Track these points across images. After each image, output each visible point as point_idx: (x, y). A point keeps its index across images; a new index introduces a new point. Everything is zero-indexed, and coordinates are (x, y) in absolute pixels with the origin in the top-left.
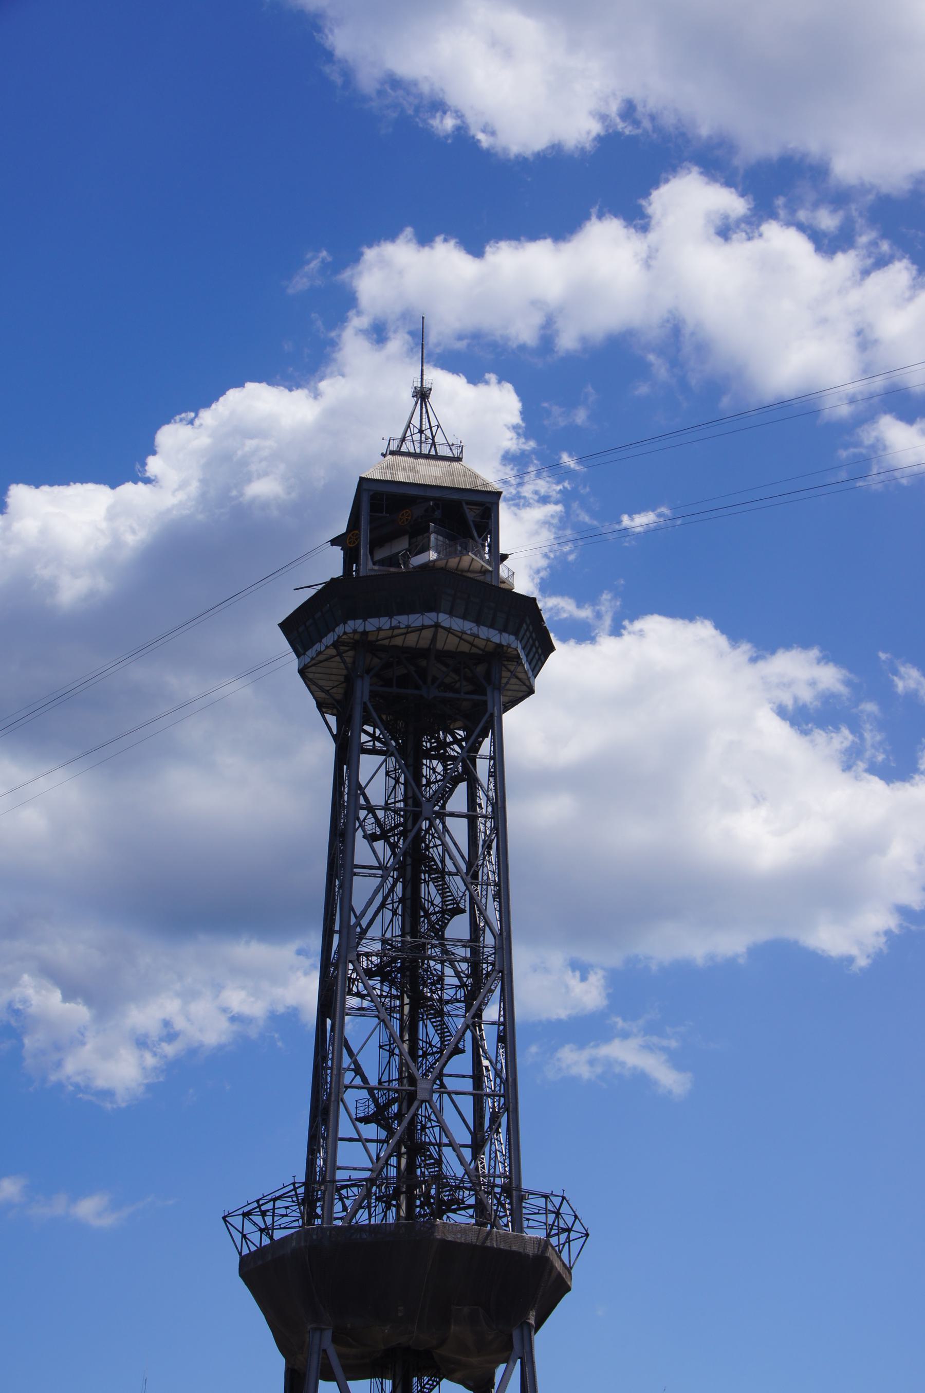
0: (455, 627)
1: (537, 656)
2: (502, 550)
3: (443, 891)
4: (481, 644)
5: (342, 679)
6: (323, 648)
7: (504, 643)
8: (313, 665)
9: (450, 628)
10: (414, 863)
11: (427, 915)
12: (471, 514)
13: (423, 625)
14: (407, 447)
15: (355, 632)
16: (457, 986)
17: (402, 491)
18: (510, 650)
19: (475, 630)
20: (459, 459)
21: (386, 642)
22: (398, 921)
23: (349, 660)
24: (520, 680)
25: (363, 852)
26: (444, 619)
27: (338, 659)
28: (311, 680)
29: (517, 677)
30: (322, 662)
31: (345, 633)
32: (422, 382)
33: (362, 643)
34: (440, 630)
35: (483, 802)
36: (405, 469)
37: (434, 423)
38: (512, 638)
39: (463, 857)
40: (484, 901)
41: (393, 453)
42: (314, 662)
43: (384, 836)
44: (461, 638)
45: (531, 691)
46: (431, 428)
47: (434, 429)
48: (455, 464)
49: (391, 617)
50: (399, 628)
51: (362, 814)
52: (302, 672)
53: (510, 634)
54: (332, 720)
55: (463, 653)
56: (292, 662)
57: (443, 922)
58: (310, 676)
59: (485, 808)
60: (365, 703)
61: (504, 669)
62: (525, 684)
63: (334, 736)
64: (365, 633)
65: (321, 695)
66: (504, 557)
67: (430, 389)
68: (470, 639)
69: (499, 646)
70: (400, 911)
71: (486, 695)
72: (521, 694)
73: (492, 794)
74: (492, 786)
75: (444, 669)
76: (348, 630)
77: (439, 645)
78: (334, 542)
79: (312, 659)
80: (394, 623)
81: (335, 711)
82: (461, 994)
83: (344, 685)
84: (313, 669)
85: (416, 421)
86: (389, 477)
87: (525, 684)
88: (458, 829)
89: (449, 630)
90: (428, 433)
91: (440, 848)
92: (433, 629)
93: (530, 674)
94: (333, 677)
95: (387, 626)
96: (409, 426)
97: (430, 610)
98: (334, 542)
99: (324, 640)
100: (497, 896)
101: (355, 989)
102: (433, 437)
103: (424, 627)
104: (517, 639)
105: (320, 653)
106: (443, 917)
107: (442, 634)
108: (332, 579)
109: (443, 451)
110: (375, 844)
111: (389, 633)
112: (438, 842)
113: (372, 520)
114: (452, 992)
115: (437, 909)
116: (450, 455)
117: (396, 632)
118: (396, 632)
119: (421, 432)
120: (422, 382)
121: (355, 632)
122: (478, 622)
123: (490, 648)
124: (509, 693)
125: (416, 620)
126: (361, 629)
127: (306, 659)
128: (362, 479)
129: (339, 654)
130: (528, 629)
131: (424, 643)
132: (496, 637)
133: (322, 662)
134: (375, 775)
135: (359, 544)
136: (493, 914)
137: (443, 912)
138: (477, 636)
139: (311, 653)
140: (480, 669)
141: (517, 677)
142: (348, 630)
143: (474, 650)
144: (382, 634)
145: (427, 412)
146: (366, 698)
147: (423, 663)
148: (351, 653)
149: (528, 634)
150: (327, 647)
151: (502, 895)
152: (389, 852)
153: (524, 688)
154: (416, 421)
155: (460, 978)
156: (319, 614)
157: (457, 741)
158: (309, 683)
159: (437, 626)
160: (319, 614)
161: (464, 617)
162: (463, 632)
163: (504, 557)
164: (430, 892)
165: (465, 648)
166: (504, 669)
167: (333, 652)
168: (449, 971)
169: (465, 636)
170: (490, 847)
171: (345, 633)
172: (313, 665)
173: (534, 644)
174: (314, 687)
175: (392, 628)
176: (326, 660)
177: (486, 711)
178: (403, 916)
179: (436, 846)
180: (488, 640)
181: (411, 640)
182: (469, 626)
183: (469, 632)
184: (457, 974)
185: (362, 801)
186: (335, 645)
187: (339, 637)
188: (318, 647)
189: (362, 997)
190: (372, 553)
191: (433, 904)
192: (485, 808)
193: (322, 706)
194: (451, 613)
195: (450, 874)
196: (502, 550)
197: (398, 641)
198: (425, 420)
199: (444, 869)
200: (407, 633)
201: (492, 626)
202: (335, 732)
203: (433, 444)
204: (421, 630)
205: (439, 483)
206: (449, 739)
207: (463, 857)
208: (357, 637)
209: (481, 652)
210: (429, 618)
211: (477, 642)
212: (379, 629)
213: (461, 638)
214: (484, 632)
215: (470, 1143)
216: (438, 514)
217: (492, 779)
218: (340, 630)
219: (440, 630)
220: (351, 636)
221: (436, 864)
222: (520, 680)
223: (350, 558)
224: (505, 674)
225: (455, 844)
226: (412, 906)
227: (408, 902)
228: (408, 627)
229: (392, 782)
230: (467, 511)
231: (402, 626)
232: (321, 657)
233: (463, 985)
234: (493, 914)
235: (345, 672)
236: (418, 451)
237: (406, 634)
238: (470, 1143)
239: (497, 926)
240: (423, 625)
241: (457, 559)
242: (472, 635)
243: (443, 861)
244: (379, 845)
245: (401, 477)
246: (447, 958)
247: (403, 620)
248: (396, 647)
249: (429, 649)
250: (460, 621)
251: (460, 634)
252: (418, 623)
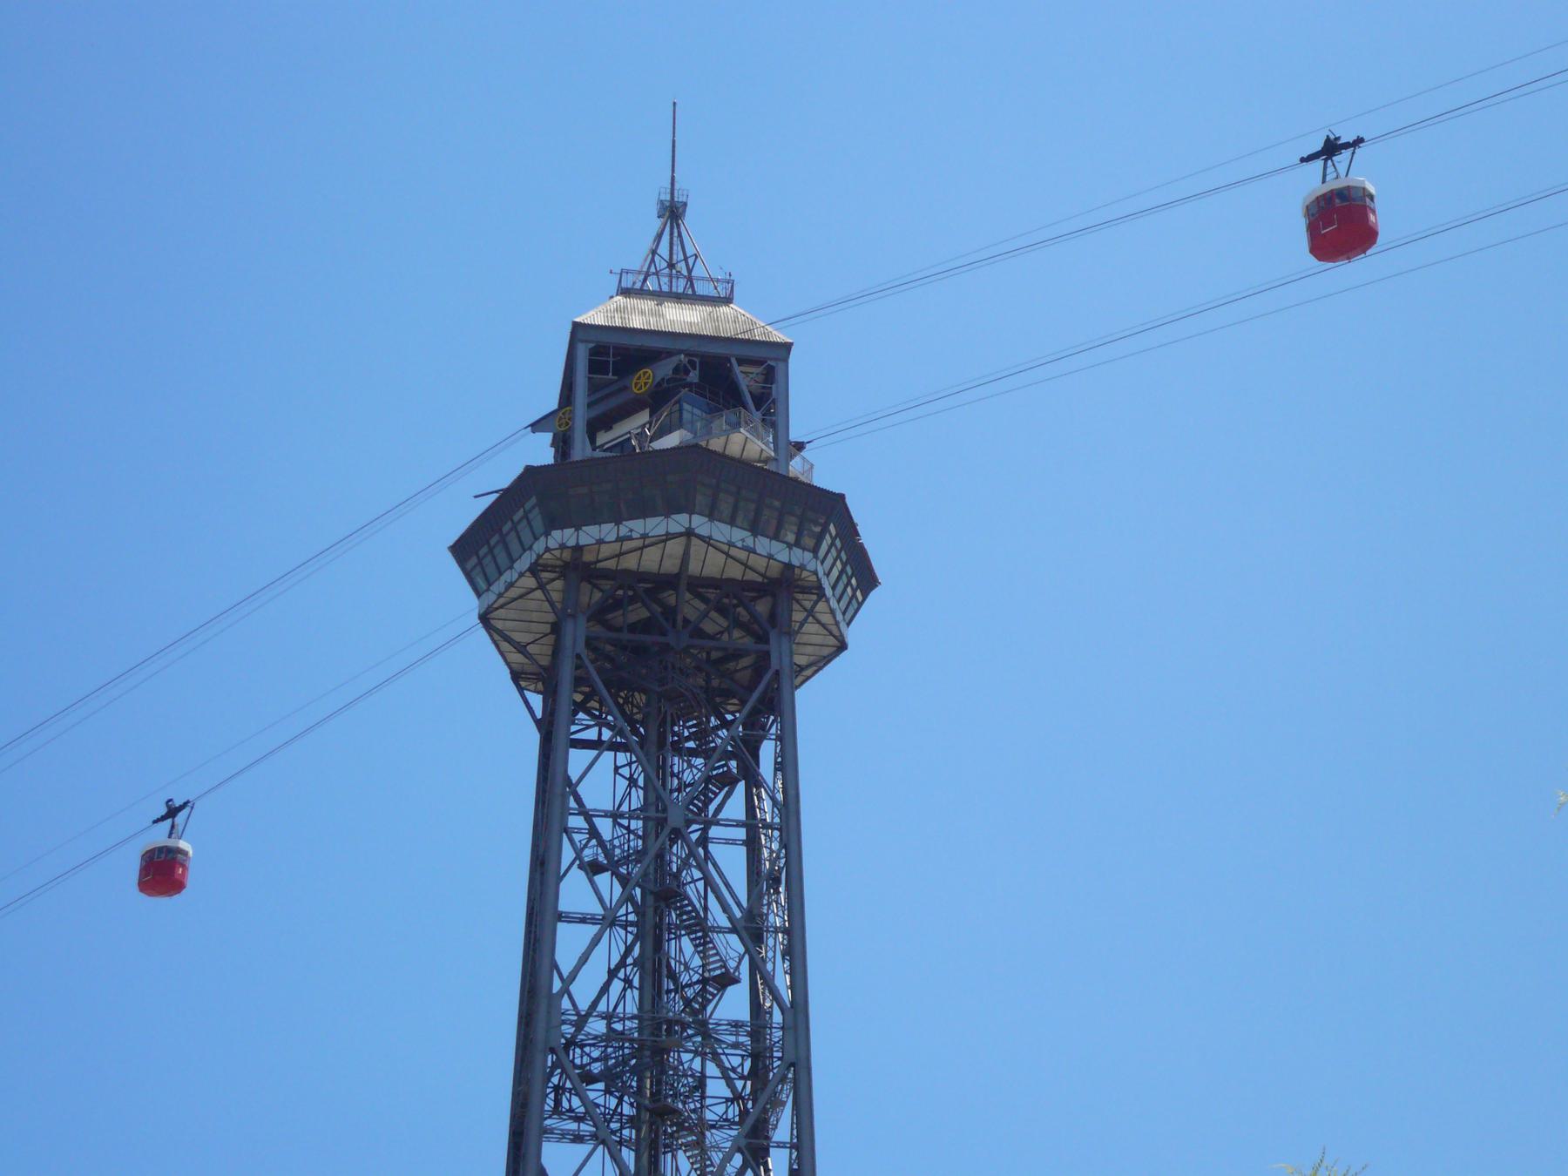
0: (717, 536)
1: (844, 578)
2: (795, 435)
3: (703, 944)
4: (759, 563)
5: (547, 628)
6: (515, 576)
7: (796, 562)
8: (501, 607)
9: (710, 538)
10: (657, 903)
11: (679, 988)
12: (746, 378)
13: (667, 534)
14: (651, 285)
15: (563, 547)
16: (727, 1100)
17: (637, 342)
18: (805, 574)
19: (750, 542)
20: (728, 300)
21: (611, 564)
22: (632, 997)
23: (556, 596)
24: (824, 626)
25: (575, 893)
26: (700, 524)
27: (538, 594)
28: (500, 633)
29: (819, 622)
30: (515, 599)
31: (547, 550)
32: (672, 194)
33: (577, 568)
34: (694, 541)
35: (767, 805)
36: (643, 313)
37: (690, 251)
38: (808, 555)
39: (739, 904)
40: (769, 966)
41: (626, 292)
42: (502, 601)
43: (612, 866)
44: (727, 554)
45: (842, 646)
46: (686, 259)
47: (691, 261)
48: (724, 309)
49: (618, 522)
50: (630, 538)
51: (576, 822)
52: (485, 619)
53: (804, 549)
54: (537, 701)
55: (732, 581)
56: (467, 603)
57: (704, 998)
58: (499, 625)
59: (767, 811)
60: (578, 656)
61: (796, 606)
62: (831, 634)
63: (538, 722)
64: (578, 548)
65: (517, 658)
66: (800, 446)
67: (685, 204)
68: (742, 555)
69: (788, 567)
70: (636, 983)
71: (767, 641)
72: (826, 651)
73: (780, 797)
74: (779, 784)
75: (702, 606)
76: (552, 544)
77: (694, 568)
78: (536, 426)
79: (500, 595)
80: (623, 531)
81: (540, 686)
82: (733, 1112)
83: (552, 637)
84: (501, 613)
85: (664, 249)
86: (618, 323)
87: (831, 634)
88: (731, 861)
89: (707, 540)
90: (682, 267)
91: (700, 885)
92: (683, 540)
93: (839, 617)
94: (534, 627)
95: (612, 537)
96: (653, 260)
97: (679, 512)
98: (536, 426)
99: (516, 565)
100: (788, 952)
101: (565, 1104)
102: (690, 271)
103: (669, 536)
104: (816, 557)
105: (510, 585)
106: (704, 990)
107: (697, 547)
108: (530, 471)
109: (702, 288)
110: (599, 879)
111: (616, 547)
112: (697, 874)
113: (593, 388)
114: (720, 1109)
115: (695, 978)
116: (714, 293)
117: (628, 545)
118: (628, 545)
119: (671, 266)
120: (672, 194)
121: (563, 547)
122: (755, 530)
123: (775, 570)
124: (809, 649)
125: (656, 526)
126: (572, 543)
127: (490, 597)
128: (577, 327)
129: (541, 586)
130: (833, 544)
131: (671, 566)
132: (783, 554)
133: (515, 599)
134: (602, 780)
135: (571, 429)
136: (782, 981)
137: (704, 981)
138: (752, 551)
139: (498, 587)
140: (762, 607)
141: (819, 622)
142: (552, 544)
143: (751, 576)
144: (606, 550)
145: (680, 235)
146: (581, 648)
147: (670, 597)
148: (558, 584)
149: (833, 551)
150: (521, 575)
151: (795, 953)
152: (618, 889)
153: (832, 641)
154: (664, 249)
155: (730, 1083)
156: (509, 525)
157: (726, 724)
158: (497, 637)
159: (689, 533)
160: (509, 525)
161: (732, 522)
162: (731, 544)
163: (800, 446)
164: (684, 949)
165: (735, 572)
166: (796, 606)
167: (530, 582)
168: (712, 1069)
169: (733, 552)
170: (777, 881)
171: (547, 550)
172: (501, 607)
173: (842, 572)
174: (505, 646)
175: (620, 539)
176: (521, 597)
177: (768, 667)
178: (641, 989)
179: (694, 881)
180: (770, 557)
181: (650, 560)
182: (739, 535)
183: (739, 544)
184: (725, 1074)
185: (572, 804)
186: (534, 570)
187: (539, 557)
188: (507, 577)
189: (579, 1119)
190: (593, 440)
191: (687, 968)
192: (767, 811)
193: (516, 677)
194: (712, 516)
195: (721, 930)
196: (795, 435)
197: (630, 563)
198: (677, 248)
199: (706, 918)
200: (645, 546)
201: (776, 537)
202: (539, 715)
203: (690, 279)
204: (665, 541)
205: (694, 331)
206: (714, 721)
207: (739, 904)
208: (567, 555)
209: (760, 579)
210: (678, 523)
211: (754, 560)
212: (600, 542)
213: (727, 554)
214: (763, 545)
215: (562, 928)
216: (694, 376)
217: (779, 775)
218: (539, 546)
219: (694, 541)
220: (557, 553)
221: (691, 903)
222: (824, 626)
223: (562, 444)
224: (798, 616)
225: (727, 885)
226: (654, 969)
227: (649, 965)
228: (644, 536)
229: (622, 784)
230: (741, 377)
231: (635, 535)
232: (513, 593)
233: (737, 1097)
234: (782, 981)
235: (551, 618)
236: (665, 288)
237: (641, 549)
238: (562, 928)
239: (787, 995)
240: (667, 534)
241: (723, 439)
242: (744, 548)
243: (706, 909)
244: (603, 879)
245: (637, 322)
246: (709, 1047)
247: (637, 526)
248: (626, 572)
249: (677, 576)
250: (725, 528)
251: (726, 548)
252: (661, 530)
